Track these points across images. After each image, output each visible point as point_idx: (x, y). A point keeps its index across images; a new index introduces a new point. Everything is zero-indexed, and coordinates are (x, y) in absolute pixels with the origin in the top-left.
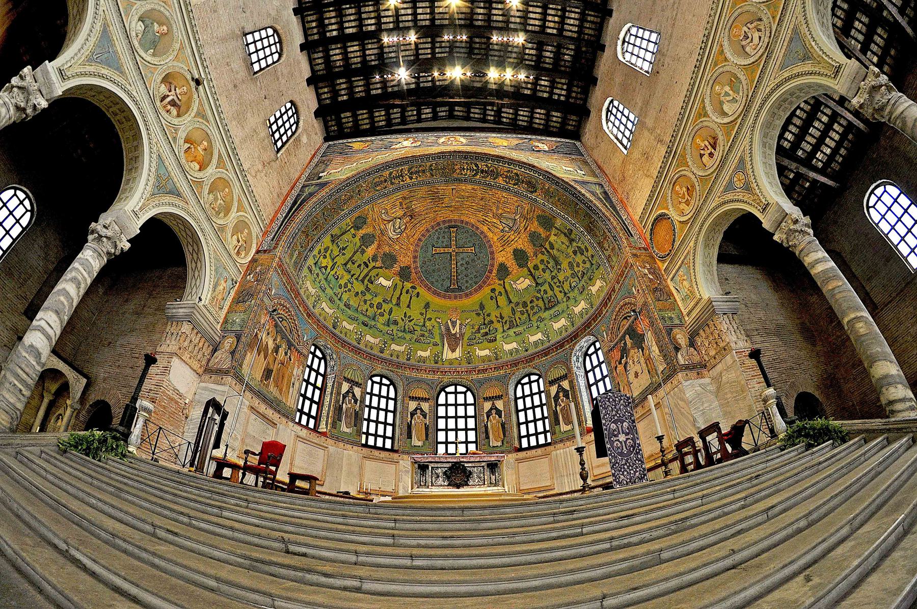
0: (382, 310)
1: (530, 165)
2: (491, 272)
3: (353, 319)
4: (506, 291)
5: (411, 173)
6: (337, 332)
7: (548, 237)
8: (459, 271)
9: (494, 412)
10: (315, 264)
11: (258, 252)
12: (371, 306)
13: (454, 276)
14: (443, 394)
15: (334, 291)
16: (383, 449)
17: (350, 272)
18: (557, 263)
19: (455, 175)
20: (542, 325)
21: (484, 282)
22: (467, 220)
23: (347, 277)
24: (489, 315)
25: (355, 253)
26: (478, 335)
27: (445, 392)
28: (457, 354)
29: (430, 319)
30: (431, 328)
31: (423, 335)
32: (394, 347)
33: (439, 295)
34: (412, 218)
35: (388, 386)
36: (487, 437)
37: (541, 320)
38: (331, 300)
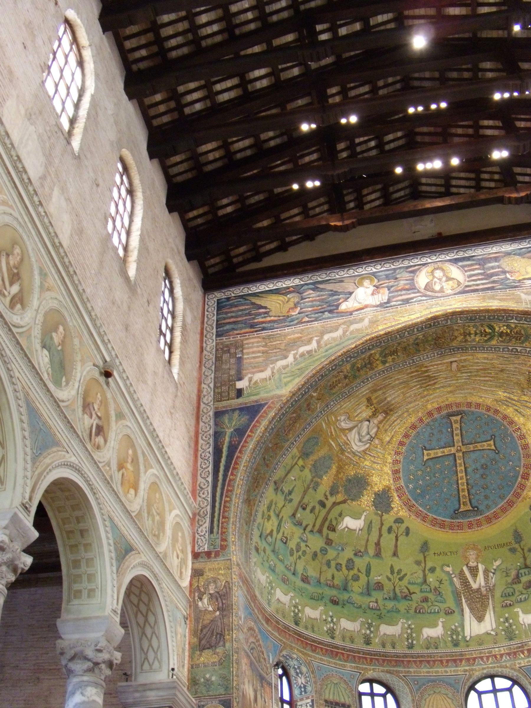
0: (355, 571)
3: (316, 599)
5: (385, 356)
6: (301, 629)
8: (471, 482)
10: (260, 536)
11: (196, 556)
12: (338, 567)
13: (463, 490)
14: (473, 694)
15: (286, 563)
17: (301, 525)
19: (455, 344)
21: (517, 495)
22: (480, 401)
23: (298, 531)
25: (305, 492)
26: (519, 587)
27: (476, 691)
29: (433, 570)
30: (437, 584)
32: (385, 629)
33: (442, 525)
34: (387, 414)
35: (384, 696)
38: (285, 581)
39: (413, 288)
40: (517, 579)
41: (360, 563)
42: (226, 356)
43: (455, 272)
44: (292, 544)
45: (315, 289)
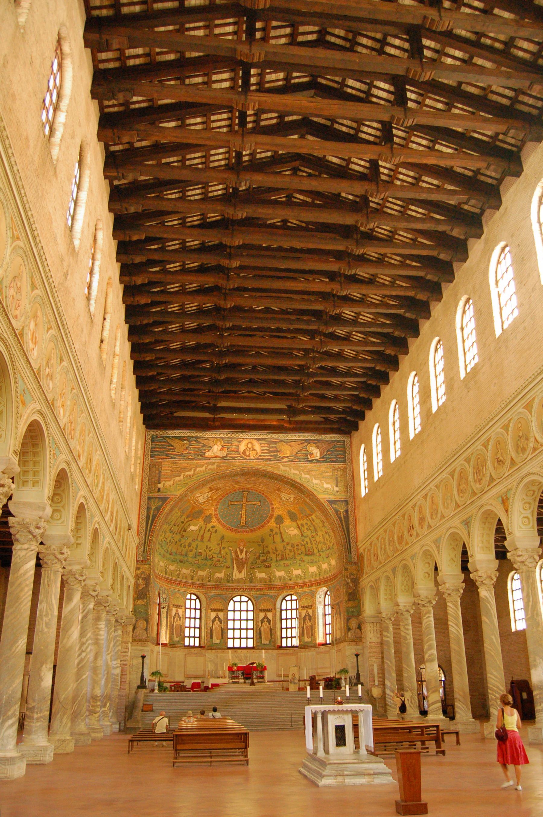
1: (301, 484)
2: (271, 518)
4: (281, 533)
6: (167, 576)
7: (311, 515)
9: (266, 620)
11: (137, 561)
14: (232, 602)
16: (194, 647)
18: (316, 530)
20: (302, 564)
21: (266, 524)
23: (171, 535)
24: (267, 547)
26: (259, 561)
28: (243, 575)
29: (224, 548)
31: (219, 561)
32: (200, 573)
33: (232, 530)
35: (195, 600)
36: (261, 637)
37: (303, 561)
39: (237, 451)
40: (259, 558)
41: (194, 544)
42: (154, 469)
43: (257, 446)
44: (168, 541)
45: (196, 441)
